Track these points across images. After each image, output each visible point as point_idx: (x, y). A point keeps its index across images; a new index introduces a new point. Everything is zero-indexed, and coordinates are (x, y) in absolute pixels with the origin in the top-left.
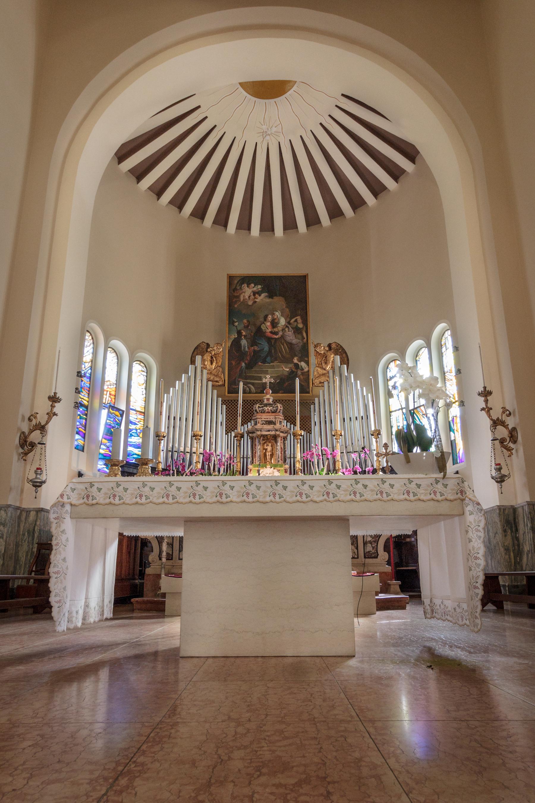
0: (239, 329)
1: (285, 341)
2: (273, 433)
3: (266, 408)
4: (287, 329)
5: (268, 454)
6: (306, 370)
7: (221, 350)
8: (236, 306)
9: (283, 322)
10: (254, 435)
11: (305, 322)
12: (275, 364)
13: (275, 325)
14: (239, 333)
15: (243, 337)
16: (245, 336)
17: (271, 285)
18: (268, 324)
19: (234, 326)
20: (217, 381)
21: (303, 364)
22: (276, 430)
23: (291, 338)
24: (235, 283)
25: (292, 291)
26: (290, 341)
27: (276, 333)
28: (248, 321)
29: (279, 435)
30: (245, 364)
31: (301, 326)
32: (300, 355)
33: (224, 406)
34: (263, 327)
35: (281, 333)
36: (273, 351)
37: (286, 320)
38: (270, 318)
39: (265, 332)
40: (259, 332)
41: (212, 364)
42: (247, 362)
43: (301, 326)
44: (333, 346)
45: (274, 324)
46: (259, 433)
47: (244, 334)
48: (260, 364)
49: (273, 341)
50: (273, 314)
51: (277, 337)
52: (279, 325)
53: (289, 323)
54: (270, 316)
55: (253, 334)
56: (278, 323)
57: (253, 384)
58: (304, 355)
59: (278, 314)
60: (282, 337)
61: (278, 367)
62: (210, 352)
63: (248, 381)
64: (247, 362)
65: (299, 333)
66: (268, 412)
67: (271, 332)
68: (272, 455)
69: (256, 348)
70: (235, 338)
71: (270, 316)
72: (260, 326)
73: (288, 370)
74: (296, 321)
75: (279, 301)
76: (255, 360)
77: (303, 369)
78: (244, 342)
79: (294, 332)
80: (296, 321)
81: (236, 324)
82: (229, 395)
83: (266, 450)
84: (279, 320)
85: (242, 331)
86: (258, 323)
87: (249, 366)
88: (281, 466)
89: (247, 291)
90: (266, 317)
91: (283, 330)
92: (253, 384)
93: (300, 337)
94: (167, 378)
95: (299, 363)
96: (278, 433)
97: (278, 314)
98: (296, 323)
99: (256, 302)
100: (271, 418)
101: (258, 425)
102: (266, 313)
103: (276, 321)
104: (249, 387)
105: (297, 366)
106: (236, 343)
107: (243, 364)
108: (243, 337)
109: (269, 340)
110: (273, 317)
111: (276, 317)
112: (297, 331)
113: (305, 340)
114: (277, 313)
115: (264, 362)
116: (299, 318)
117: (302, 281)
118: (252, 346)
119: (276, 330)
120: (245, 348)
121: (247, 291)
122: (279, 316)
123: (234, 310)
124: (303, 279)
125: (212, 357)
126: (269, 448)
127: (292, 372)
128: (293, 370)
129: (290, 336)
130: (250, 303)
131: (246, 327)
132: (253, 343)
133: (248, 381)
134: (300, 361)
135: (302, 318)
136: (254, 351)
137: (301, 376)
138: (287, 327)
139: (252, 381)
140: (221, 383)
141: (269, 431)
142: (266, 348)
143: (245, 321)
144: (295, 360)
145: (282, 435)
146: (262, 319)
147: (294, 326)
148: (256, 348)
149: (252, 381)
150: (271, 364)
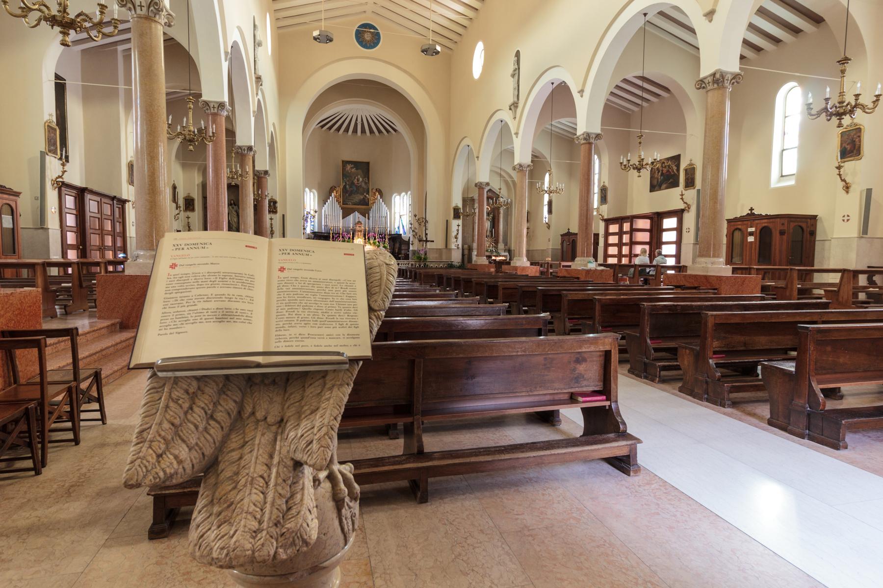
7: (340, 189)
17: (356, 164)
24: (345, 163)
25: (364, 167)
40: (353, 183)
45: (358, 180)
58: (368, 193)
75: (360, 171)
76: (351, 193)
87: (350, 195)
89: (349, 167)
94: (323, 201)
106: (345, 187)
112: (366, 183)
117: (368, 163)
121: (349, 167)
123: (345, 175)
124: (368, 163)
129: (363, 184)
132: (351, 187)
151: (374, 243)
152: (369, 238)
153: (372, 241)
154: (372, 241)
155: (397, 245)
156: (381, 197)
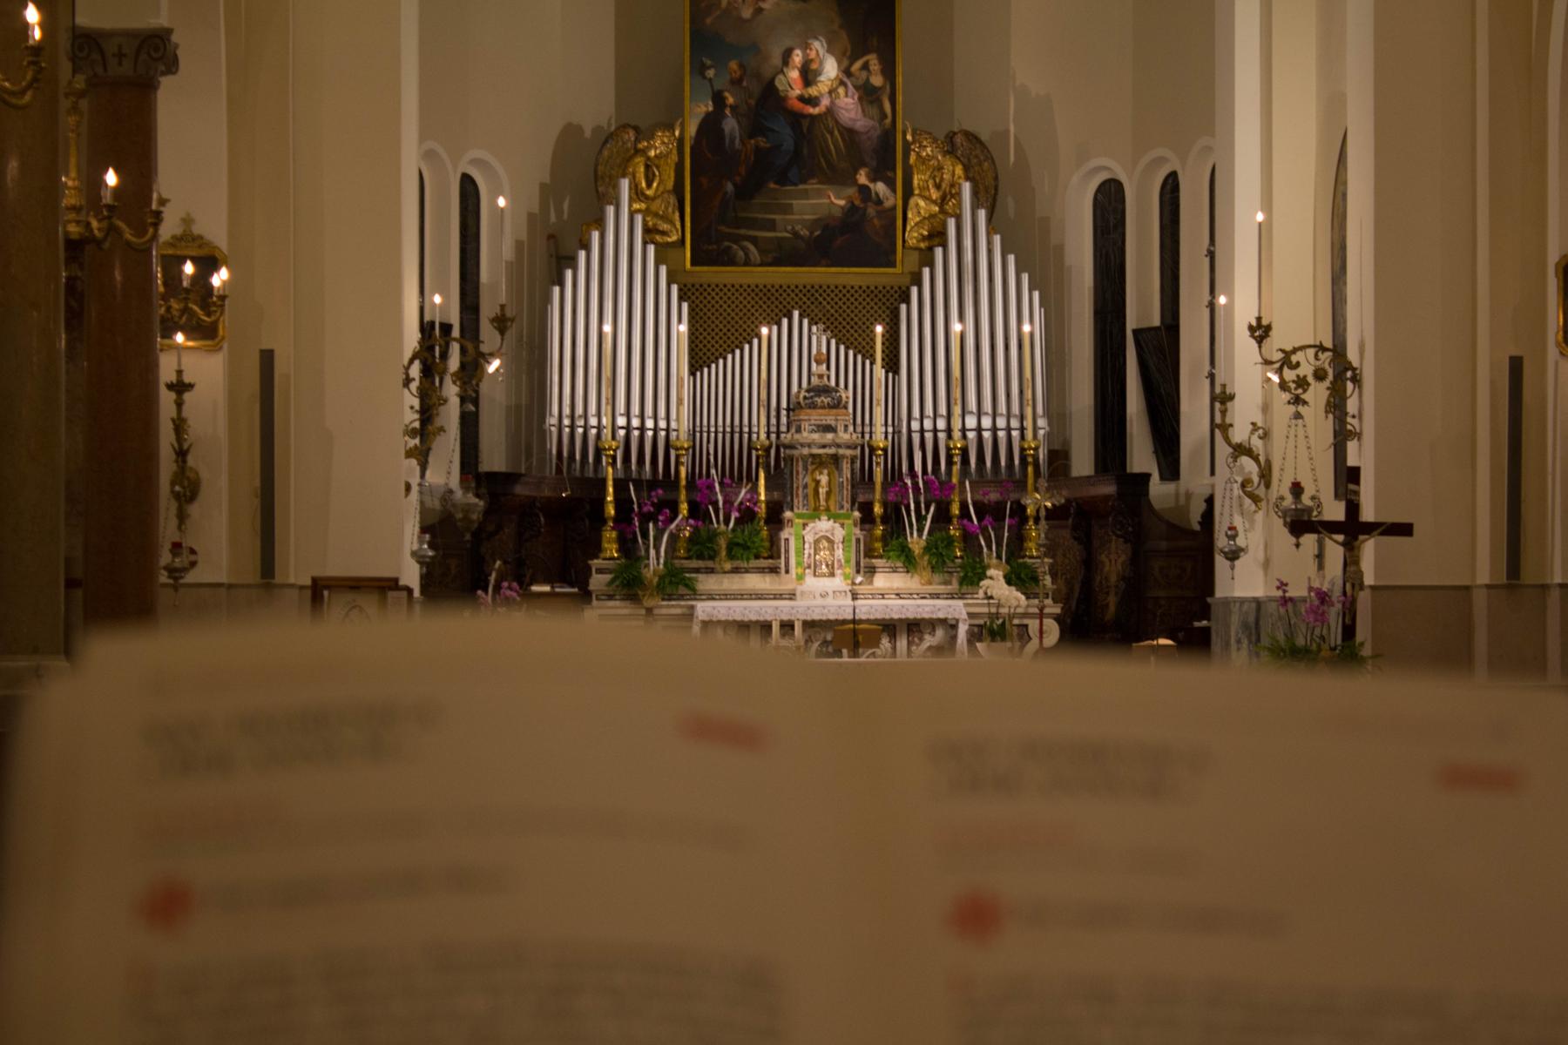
0: (717, 87)
1: (837, 122)
2: (832, 451)
3: (818, 400)
4: (841, 90)
5: (822, 491)
6: (888, 204)
8: (709, 21)
9: (830, 69)
10: (796, 453)
11: (889, 71)
12: (812, 185)
13: (810, 77)
14: (718, 99)
15: (728, 111)
16: (734, 108)
18: (794, 74)
19: (704, 77)
20: (664, 233)
21: (880, 187)
22: (839, 446)
23: (852, 115)
26: (849, 124)
27: (813, 101)
28: (741, 66)
29: (844, 456)
30: (735, 185)
31: (877, 80)
32: (874, 163)
33: (685, 306)
34: (780, 83)
35: (825, 102)
36: (805, 151)
37: (839, 62)
38: (798, 57)
39: (785, 99)
40: (770, 95)
41: (649, 185)
42: (738, 179)
43: (877, 80)
44: (959, 139)
45: (809, 75)
46: (806, 451)
47: (731, 100)
48: (772, 185)
49: (805, 124)
50: (806, 47)
51: (815, 111)
52: (822, 78)
53: (847, 72)
54: (798, 52)
55: (753, 102)
56: (818, 73)
57: (754, 240)
59: (816, 45)
60: (830, 111)
61: (819, 194)
62: (644, 152)
63: (743, 232)
64: (738, 179)
65: (871, 102)
66: (823, 407)
67: (801, 99)
68: (828, 494)
69: (762, 142)
70: (708, 115)
71: (798, 52)
72: (773, 80)
73: (842, 203)
74: (865, 67)
77: (879, 202)
78: (730, 125)
79: (860, 99)
80: (865, 67)
81: (711, 73)
82: (698, 268)
83: (818, 482)
84: (821, 63)
85: (727, 94)
86: (767, 74)
87: (747, 191)
88: (848, 517)
90: (787, 54)
91: (830, 92)
92: (754, 240)
93: (874, 111)
95: (871, 186)
96: (841, 451)
97: (818, 46)
98: (864, 74)
99: (760, 10)
100: (830, 420)
101: (805, 434)
102: (788, 43)
103: (814, 66)
104: (744, 249)
105: (864, 190)
106: (710, 125)
107: (730, 187)
108: (728, 111)
109: (796, 119)
110: (805, 55)
111: (813, 55)
112: (868, 95)
113: (888, 121)
114: (816, 45)
115: (783, 180)
116: (873, 60)
118: (751, 136)
119: (813, 91)
120: (732, 140)
122: (821, 53)
125: (647, 167)
126: (824, 479)
127: (852, 209)
128: (857, 203)
130: (747, 13)
131: (737, 82)
132: (755, 127)
133: (743, 232)
134: (874, 180)
135: (881, 60)
136: (758, 149)
137: (876, 221)
138: (842, 83)
139: (752, 233)
140: (674, 238)
141: (824, 447)
142: (788, 143)
143: (733, 65)
144: (862, 178)
145: (849, 452)
146: (776, 60)
147: (861, 82)
148: (762, 142)
149: (752, 233)
150: (801, 187)
151: (938, 556)
152: (895, 518)
153: (916, 542)
154: (916, 542)
155: (1114, 562)
156: (988, 196)
